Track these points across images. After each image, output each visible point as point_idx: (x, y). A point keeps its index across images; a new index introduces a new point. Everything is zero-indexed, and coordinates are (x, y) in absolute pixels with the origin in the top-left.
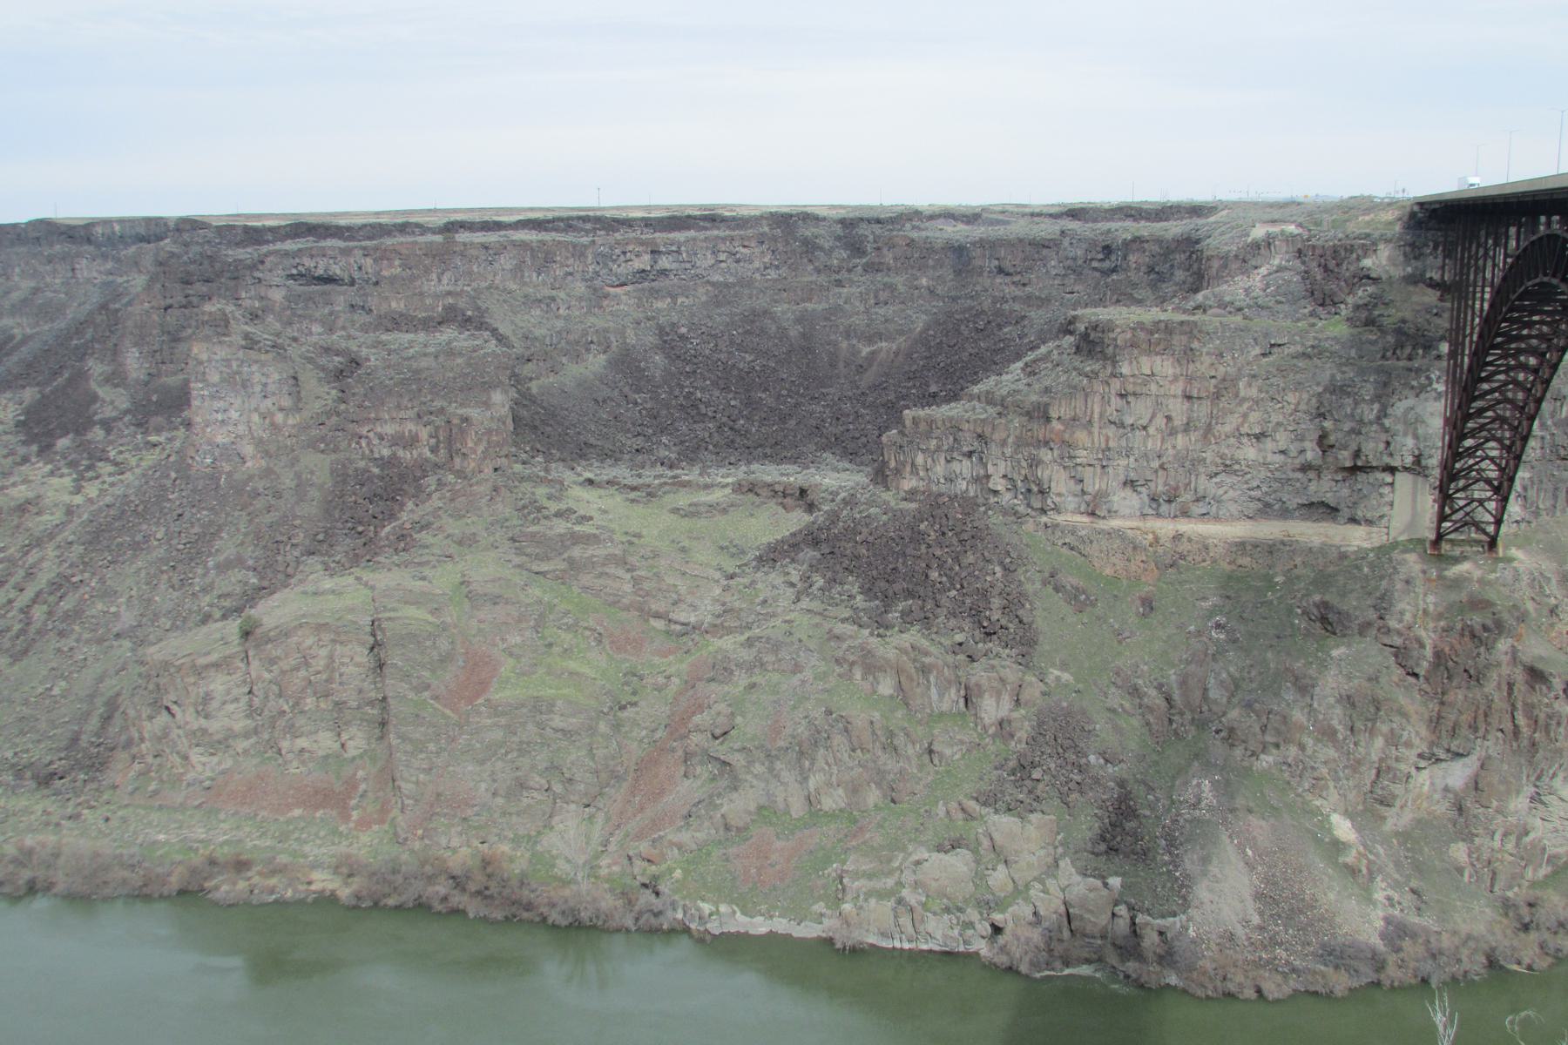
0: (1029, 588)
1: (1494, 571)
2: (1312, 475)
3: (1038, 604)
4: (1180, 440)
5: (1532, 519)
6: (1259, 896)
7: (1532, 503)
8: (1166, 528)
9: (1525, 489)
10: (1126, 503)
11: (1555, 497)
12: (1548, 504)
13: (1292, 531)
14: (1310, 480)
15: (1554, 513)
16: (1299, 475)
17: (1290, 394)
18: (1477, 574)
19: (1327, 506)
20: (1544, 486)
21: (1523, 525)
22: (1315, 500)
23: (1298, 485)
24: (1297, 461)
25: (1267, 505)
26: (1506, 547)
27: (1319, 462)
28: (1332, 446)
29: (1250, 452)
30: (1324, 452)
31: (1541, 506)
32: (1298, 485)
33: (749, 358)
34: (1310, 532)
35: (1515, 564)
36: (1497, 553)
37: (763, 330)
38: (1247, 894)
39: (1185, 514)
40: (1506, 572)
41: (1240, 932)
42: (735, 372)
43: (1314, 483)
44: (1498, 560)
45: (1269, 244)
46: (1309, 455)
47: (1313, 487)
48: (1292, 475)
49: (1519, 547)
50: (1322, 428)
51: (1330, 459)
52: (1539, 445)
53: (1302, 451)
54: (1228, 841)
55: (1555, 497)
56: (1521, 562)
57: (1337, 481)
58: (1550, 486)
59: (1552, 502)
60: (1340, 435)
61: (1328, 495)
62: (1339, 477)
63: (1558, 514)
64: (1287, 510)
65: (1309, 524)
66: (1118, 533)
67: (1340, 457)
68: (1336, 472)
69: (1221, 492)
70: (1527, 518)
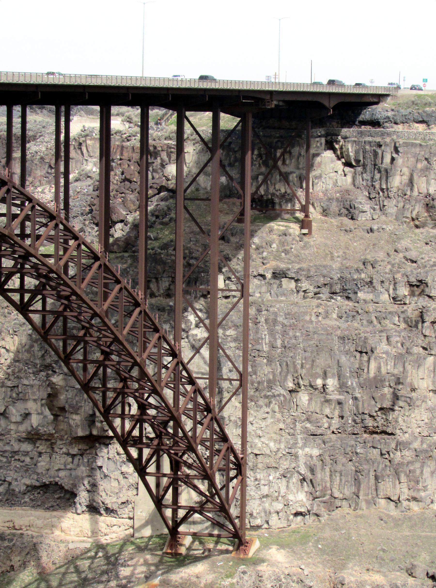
1: (230, 575)
2: (42, 447)
5: (323, 511)
7: (324, 489)
9: (312, 470)
11: (357, 482)
12: (348, 491)
13: (18, 522)
14: (40, 454)
15: (357, 504)
16: (26, 447)
17: (8, 339)
18: (210, 578)
19: (61, 488)
20: (339, 467)
21: (310, 519)
22: (46, 480)
23: (28, 460)
24: (22, 428)
26: (266, 545)
27: (51, 429)
28: (63, 409)
30: (56, 416)
31: (337, 494)
32: (28, 460)
34: (39, 523)
35: (262, 568)
36: (245, 552)
40: (246, 577)
43: (45, 459)
44: (244, 561)
45: (80, 144)
46: (35, 420)
47: (43, 463)
48: (16, 446)
49: (281, 546)
50: (51, 385)
51: (62, 426)
52: (337, 413)
53: (27, 415)
55: (357, 482)
56: (272, 564)
57: (73, 456)
58: (351, 467)
59: (353, 489)
60: (70, 395)
61: (62, 474)
62: (74, 450)
63: (363, 505)
65: (40, 513)
67: (71, 422)
68: (71, 444)
70: (315, 509)
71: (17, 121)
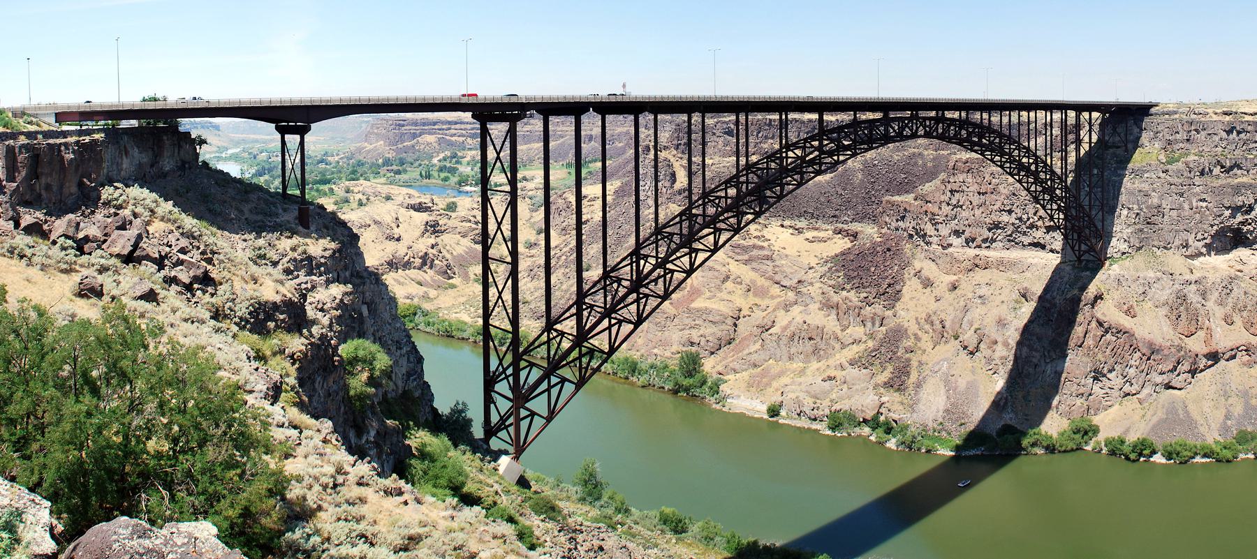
0: (906, 276)
3: (908, 283)
4: (978, 212)
6: (947, 411)
8: (972, 252)
10: (957, 241)
25: (1016, 243)
29: (1005, 218)
33: (903, 176)
37: (916, 163)
38: (942, 408)
39: (979, 247)
41: (930, 424)
42: (895, 182)
54: (943, 387)
64: (1024, 245)
66: (952, 254)
69: (995, 237)
71: (784, 117)
